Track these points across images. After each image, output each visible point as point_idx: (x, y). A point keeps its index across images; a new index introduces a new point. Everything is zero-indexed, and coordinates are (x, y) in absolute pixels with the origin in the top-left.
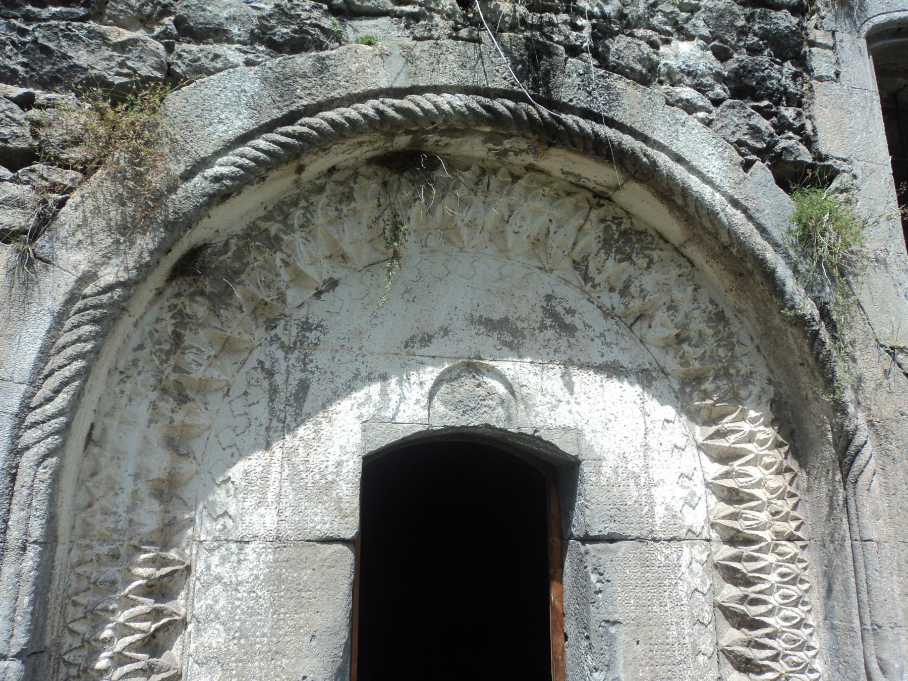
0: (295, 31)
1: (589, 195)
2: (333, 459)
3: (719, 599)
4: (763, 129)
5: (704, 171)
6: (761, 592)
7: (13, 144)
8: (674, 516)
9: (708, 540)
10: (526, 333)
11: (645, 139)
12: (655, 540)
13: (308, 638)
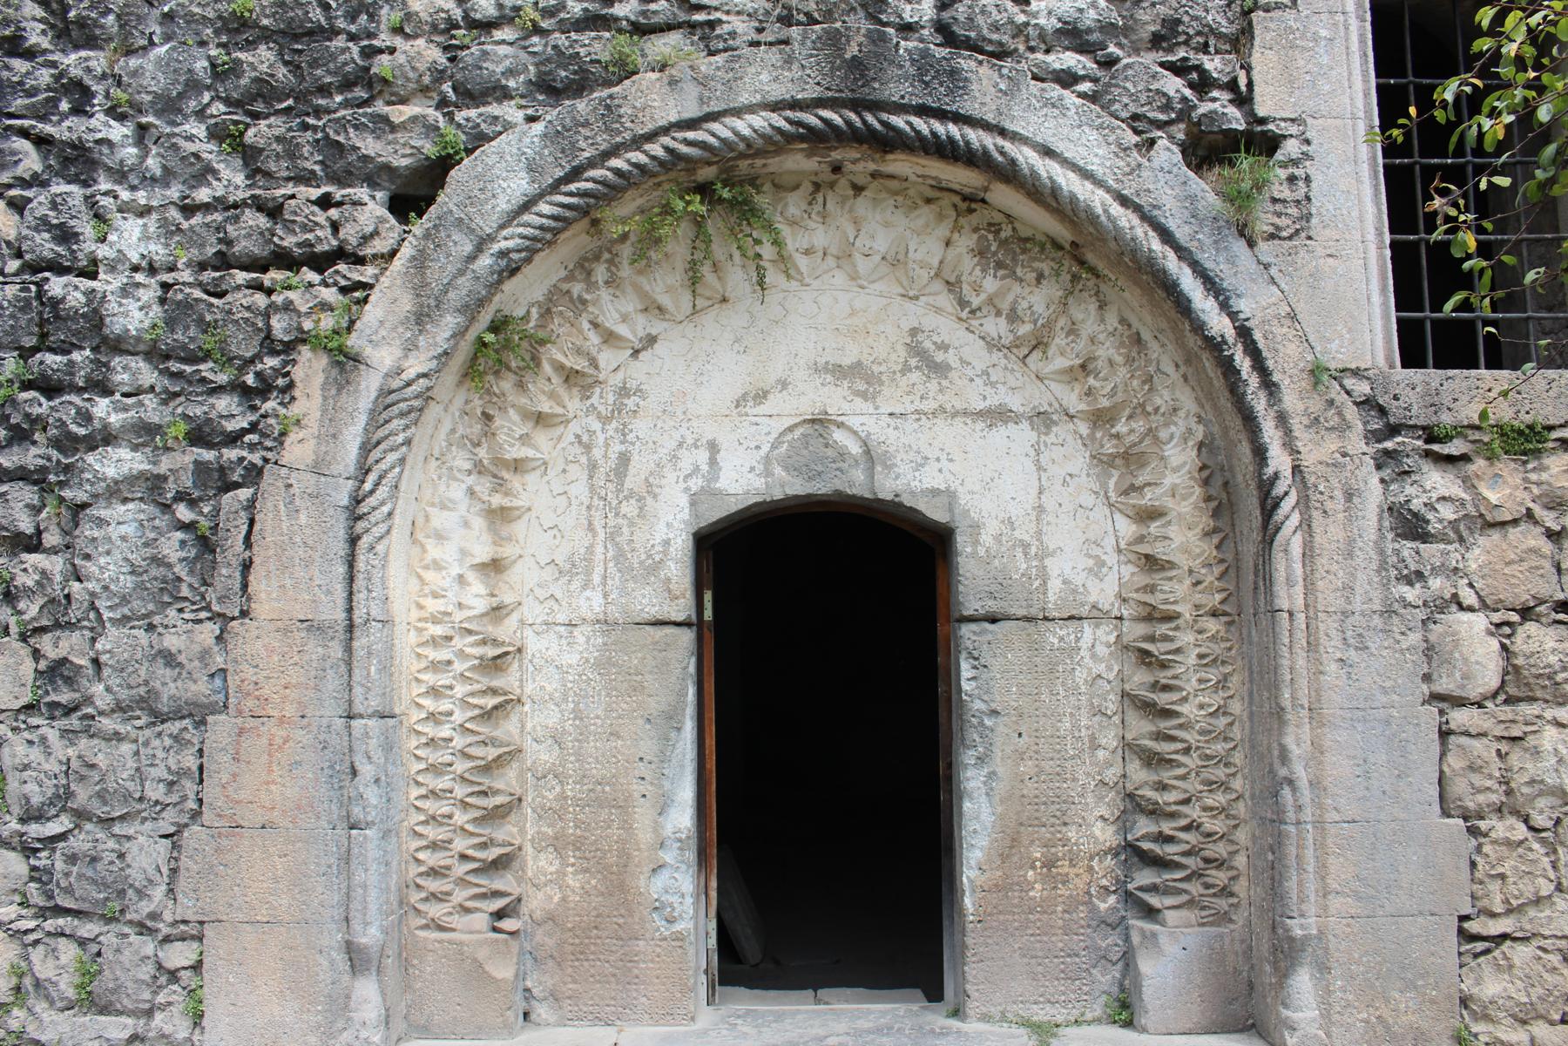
0: (575, 73)
1: (957, 199)
2: (658, 538)
3: (1127, 687)
4: (1172, 93)
5: (1081, 163)
6: (1175, 677)
7: (319, 249)
8: (1075, 591)
9: (1120, 618)
10: (884, 378)
11: (1003, 132)
12: (1046, 619)
13: (640, 721)
